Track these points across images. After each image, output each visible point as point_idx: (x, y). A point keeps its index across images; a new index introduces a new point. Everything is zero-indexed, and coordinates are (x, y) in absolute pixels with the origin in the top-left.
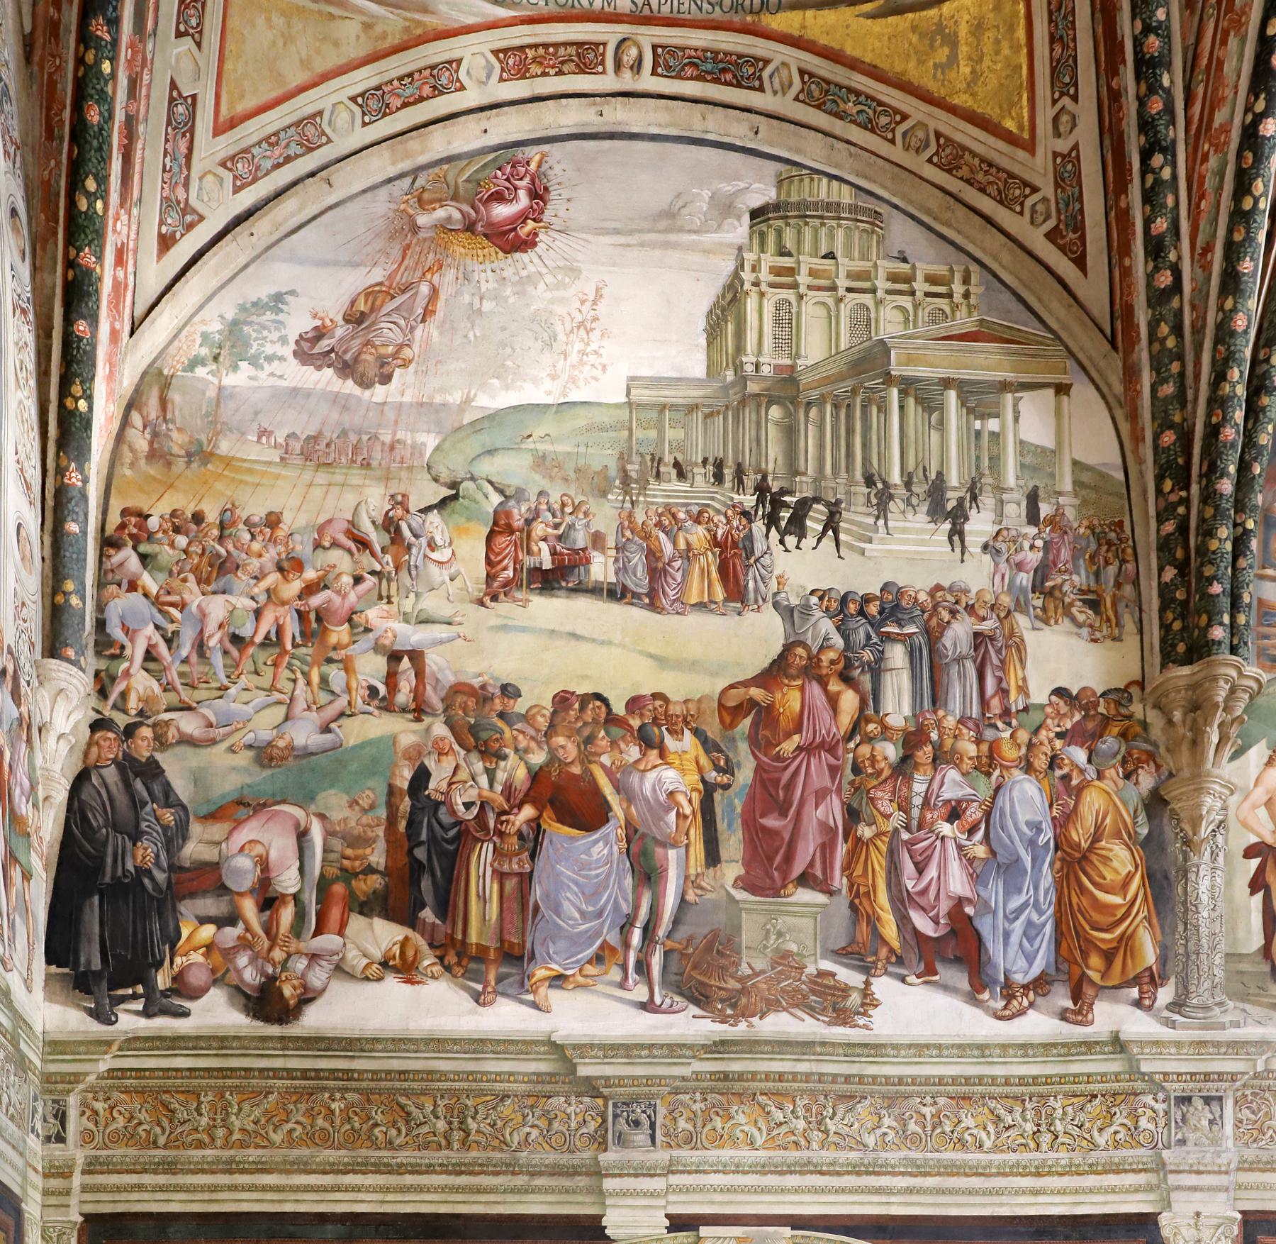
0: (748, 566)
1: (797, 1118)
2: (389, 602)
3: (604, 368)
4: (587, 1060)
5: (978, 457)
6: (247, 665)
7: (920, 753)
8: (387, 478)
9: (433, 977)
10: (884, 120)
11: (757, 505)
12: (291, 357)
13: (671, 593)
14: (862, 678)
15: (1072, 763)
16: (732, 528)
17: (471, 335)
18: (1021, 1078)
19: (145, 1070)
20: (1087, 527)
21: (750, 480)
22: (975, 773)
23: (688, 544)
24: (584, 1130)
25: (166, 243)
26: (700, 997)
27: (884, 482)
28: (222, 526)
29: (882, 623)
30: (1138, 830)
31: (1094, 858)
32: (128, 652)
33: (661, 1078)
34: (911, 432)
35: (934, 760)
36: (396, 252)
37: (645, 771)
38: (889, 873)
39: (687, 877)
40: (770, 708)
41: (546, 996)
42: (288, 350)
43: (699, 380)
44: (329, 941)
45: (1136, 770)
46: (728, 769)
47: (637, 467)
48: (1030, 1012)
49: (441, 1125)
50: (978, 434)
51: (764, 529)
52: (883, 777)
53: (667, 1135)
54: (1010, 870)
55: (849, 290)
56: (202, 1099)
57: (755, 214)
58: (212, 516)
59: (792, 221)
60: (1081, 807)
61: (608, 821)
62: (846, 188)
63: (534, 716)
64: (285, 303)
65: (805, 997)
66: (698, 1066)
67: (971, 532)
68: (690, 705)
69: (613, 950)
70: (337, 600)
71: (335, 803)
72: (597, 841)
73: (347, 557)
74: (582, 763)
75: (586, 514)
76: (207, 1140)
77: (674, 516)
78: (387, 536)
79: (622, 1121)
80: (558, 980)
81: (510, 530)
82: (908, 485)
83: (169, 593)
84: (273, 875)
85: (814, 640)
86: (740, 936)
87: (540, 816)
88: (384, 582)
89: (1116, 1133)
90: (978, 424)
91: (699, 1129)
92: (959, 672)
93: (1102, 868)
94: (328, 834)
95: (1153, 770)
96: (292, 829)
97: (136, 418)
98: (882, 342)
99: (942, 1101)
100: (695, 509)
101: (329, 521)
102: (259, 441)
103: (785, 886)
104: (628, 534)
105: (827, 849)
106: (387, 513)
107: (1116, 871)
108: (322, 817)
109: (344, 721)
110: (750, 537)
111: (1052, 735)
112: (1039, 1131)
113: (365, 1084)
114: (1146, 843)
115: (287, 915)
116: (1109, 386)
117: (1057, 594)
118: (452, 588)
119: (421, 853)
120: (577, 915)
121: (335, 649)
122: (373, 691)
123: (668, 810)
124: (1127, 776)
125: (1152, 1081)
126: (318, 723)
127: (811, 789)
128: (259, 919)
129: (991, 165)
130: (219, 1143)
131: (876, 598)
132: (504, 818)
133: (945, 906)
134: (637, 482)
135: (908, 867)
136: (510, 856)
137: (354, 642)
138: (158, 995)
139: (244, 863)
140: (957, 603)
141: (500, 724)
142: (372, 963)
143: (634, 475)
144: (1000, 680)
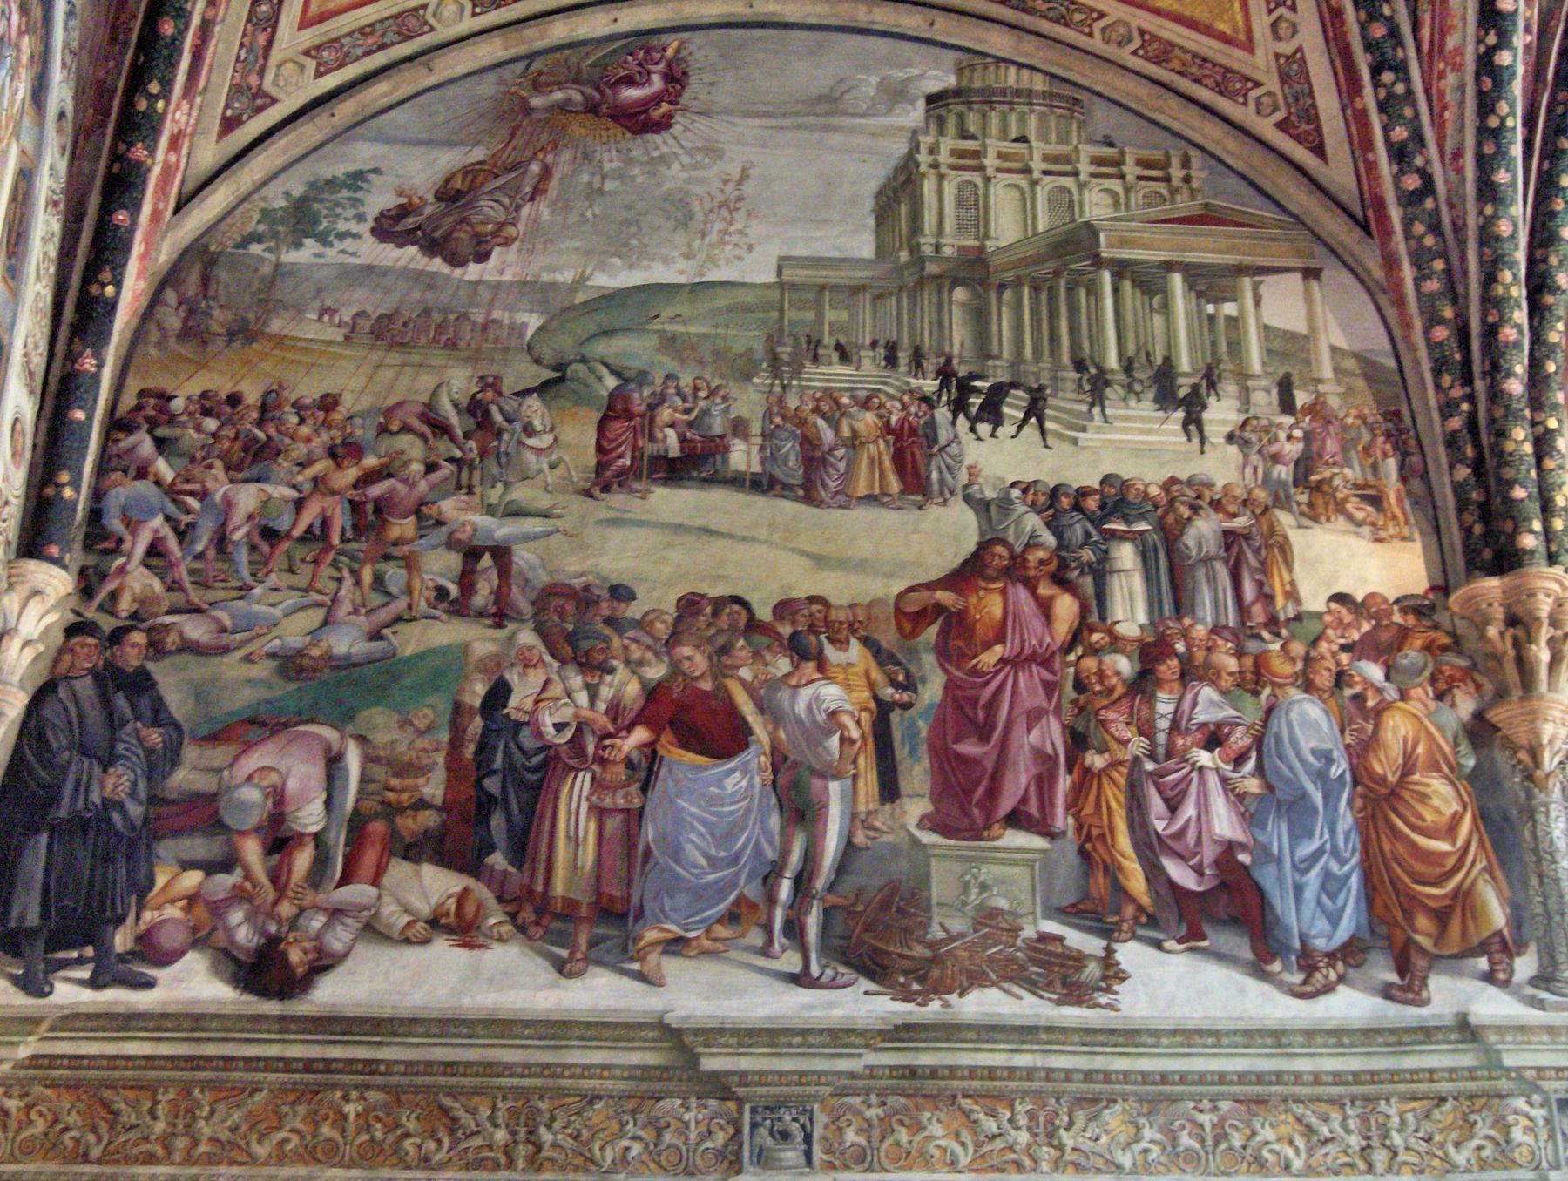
0: (931, 455)
1: (1018, 1128)
2: (470, 492)
3: (750, 248)
4: (714, 1050)
5: (1213, 343)
6: (279, 560)
7: (1163, 668)
8: (475, 358)
9: (501, 940)
10: (1078, 17)
11: (940, 390)
12: (367, 235)
13: (832, 485)
14: (1081, 581)
15: (1365, 680)
16: (909, 414)
17: (589, 214)
18: (1336, 1074)
19: (82, 1057)
20: (1356, 417)
21: (930, 365)
22: (1238, 692)
23: (854, 431)
24: (709, 1144)
25: (229, 124)
26: (875, 968)
27: (1098, 368)
28: (264, 408)
29: (1105, 518)
30: (1462, 761)
31: (1407, 795)
32: (126, 546)
33: (820, 1073)
34: (1129, 317)
35: (1183, 676)
36: (504, 132)
37: (797, 687)
38: (1130, 811)
39: (854, 816)
40: (962, 615)
41: (658, 965)
42: (364, 228)
43: (869, 261)
44: (359, 892)
45: (1450, 689)
46: (910, 685)
47: (789, 349)
48: (1341, 988)
49: (501, 1136)
50: (1212, 318)
51: (950, 416)
52: (1116, 695)
53: (828, 1151)
54: (1296, 810)
55: (1046, 173)
56: (160, 1097)
57: (931, 99)
58: (252, 394)
59: (976, 107)
60: (1382, 733)
61: (747, 745)
62: (1038, 77)
63: (651, 622)
64: (366, 181)
65: (1022, 968)
66: (872, 1058)
67: (1211, 421)
68: (858, 611)
69: (753, 906)
70: (402, 489)
71: (383, 725)
72: (733, 771)
73: (419, 443)
74: (715, 678)
75: (725, 399)
76: (160, 1152)
77: (836, 402)
78: (472, 420)
79: (763, 1131)
80: (675, 946)
81: (628, 415)
82: (1128, 367)
83: (187, 481)
84: (289, 809)
85: (1017, 538)
86: (929, 888)
87: (657, 740)
88: (465, 474)
89: (1480, 1148)
90: (1210, 308)
91: (875, 1143)
92: (1207, 575)
93: (1418, 807)
94: (369, 760)
95: (1472, 689)
96: (321, 753)
97: (170, 296)
98: (1087, 224)
99: (1225, 1106)
100: (862, 394)
101: (400, 404)
102: (320, 320)
103: (988, 827)
104: (778, 420)
105: (1044, 782)
106: (474, 395)
107: (1438, 812)
108: (362, 739)
109: (400, 627)
110: (932, 425)
111: (1335, 648)
112: (1369, 1146)
113: (394, 1080)
114: (1474, 777)
115: (303, 859)
116: (1368, 272)
117: (1326, 488)
118: (551, 477)
119: (492, 785)
120: (703, 861)
121: (395, 544)
122: (442, 593)
123: (830, 733)
124: (1440, 696)
125: (1521, 1078)
126: (367, 629)
127: (1017, 711)
128: (264, 862)
129: (1205, 60)
130: (177, 1157)
131: (1095, 491)
132: (607, 742)
133: (1209, 854)
134: (788, 364)
135: (1156, 805)
136: (614, 788)
137: (422, 537)
138: (113, 960)
139: (252, 795)
140: (1198, 497)
141: (607, 631)
142: (415, 921)
143: (785, 357)
144: (1261, 584)
